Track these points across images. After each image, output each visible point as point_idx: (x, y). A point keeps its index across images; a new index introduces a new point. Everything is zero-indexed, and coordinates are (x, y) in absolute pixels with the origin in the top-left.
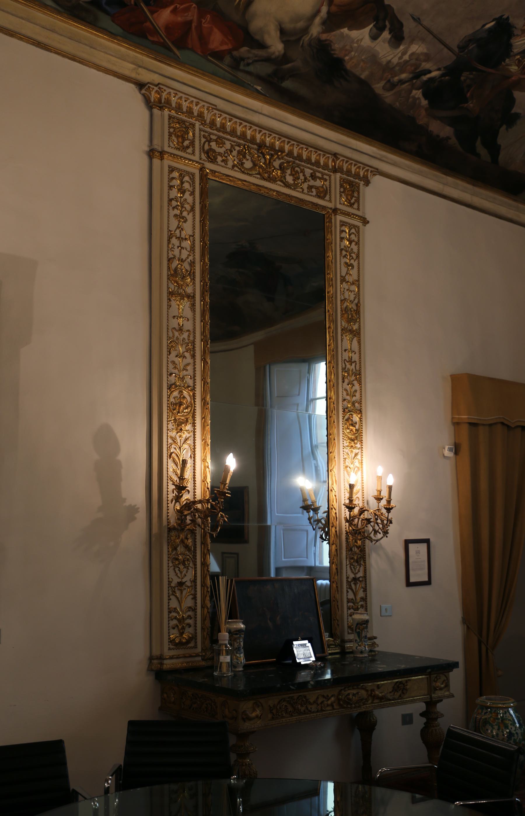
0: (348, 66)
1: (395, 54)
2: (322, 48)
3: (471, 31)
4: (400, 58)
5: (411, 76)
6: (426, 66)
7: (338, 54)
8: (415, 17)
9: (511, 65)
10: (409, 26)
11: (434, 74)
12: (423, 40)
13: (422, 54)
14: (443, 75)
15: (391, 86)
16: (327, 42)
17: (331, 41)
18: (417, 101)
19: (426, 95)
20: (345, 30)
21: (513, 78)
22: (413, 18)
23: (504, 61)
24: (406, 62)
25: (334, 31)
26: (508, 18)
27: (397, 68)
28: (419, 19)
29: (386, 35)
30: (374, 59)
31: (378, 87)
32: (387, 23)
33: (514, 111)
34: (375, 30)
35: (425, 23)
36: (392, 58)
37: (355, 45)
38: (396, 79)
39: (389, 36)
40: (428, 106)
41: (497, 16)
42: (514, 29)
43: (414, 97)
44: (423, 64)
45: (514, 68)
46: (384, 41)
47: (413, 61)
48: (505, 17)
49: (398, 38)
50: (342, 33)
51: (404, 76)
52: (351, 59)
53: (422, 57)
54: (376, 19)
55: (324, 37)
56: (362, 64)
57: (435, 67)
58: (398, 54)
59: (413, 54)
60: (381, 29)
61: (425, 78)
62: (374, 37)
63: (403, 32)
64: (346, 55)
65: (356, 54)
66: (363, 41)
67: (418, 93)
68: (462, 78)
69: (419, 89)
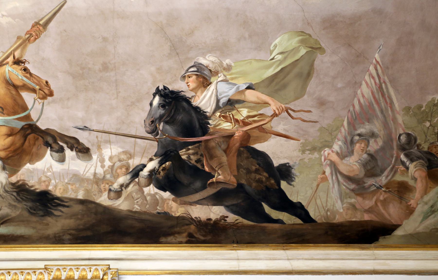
0: (58, 193)
1: (95, 165)
2: (21, 190)
3: (144, 115)
4: (103, 166)
5: (129, 177)
6: (135, 162)
7: (39, 188)
8: (80, 127)
9: (219, 124)
10: (84, 138)
11: (152, 165)
12: (109, 142)
13: (120, 154)
14: (161, 163)
15: (118, 194)
16: (20, 183)
17: (24, 180)
18: (157, 197)
19: (163, 188)
20: (28, 166)
21: (237, 134)
22: (79, 129)
23: (209, 124)
24: (112, 167)
25: (19, 170)
26: (165, 88)
27: (108, 176)
28: (85, 127)
29: (69, 153)
30: (77, 178)
31: (104, 200)
32: (61, 144)
33: (276, 163)
34: (55, 155)
35: (95, 128)
36: (95, 170)
37: (49, 174)
38: (116, 186)
39: (74, 153)
40: (173, 197)
41: (154, 91)
42: (183, 93)
43: (149, 194)
44: (131, 162)
45: (226, 126)
46: (73, 159)
47: (118, 164)
48: (161, 88)
49: (83, 151)
50: (28, 169)
51: (122, 180)
52: (56, 186)
53: (123, 157)
54: (47, 145)
55: (14, 179)
56: (70, 187)
57: (147, 160)
58: (97, 164)
59: (111, 158)
60: (61, 150)
61: (145, 172)
62: (62, 160)
63: (82, 144)
64: (48, 186)
65: (57, 181)
66: (53, 167)
67: (152, 189)
68: (184, 157)
69: (149, 185)
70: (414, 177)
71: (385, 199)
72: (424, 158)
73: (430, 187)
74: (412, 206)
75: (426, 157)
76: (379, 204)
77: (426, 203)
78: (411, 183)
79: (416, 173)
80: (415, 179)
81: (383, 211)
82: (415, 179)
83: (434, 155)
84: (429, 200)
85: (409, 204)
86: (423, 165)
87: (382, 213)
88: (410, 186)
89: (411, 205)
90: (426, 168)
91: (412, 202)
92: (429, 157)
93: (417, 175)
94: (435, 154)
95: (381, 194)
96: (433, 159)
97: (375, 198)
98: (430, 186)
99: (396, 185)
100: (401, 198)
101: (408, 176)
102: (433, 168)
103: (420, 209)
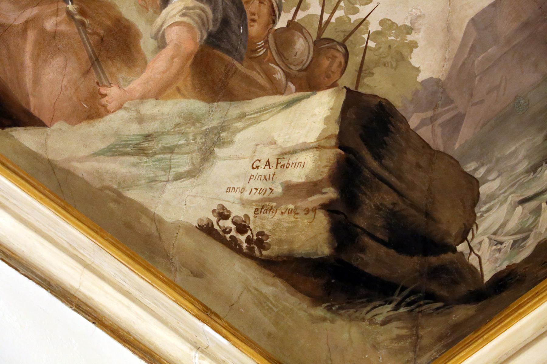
70: (163, 36)
71: (55, 35)
72: (221, 7)
73: (178, 89)
74: (104, 101)
75: (224, 9)
76: (31, 35)
77: (141, 120)
78: (147, 44)
79: (176, 29)
80: (161, 43)
81: (28, 60)
82: (162, 44)
83: (245, 18)
84: (153, 118)
85: (103, 90)
86: (203, 24)
87: (22, 64)
88: (139, 50)
89: (105, 95)
90: (205, 36)
91: (113, 93)
92: (232, 14)
93: (173, 35)
94: (249, 16)
95: (56, 13)
96: (235, 27)
97: (31, 12)
98: (180, 84)
99: (109, 23)
100: (95, 61)
101: (151, 21)
102: (218, 47)
103: (117, 123)
